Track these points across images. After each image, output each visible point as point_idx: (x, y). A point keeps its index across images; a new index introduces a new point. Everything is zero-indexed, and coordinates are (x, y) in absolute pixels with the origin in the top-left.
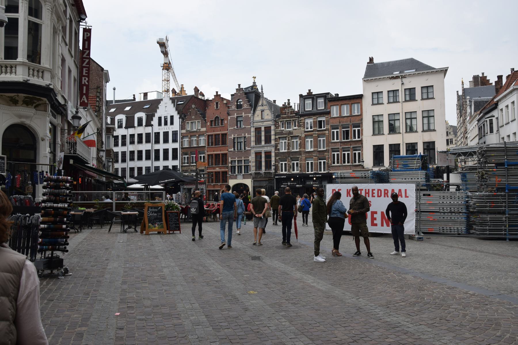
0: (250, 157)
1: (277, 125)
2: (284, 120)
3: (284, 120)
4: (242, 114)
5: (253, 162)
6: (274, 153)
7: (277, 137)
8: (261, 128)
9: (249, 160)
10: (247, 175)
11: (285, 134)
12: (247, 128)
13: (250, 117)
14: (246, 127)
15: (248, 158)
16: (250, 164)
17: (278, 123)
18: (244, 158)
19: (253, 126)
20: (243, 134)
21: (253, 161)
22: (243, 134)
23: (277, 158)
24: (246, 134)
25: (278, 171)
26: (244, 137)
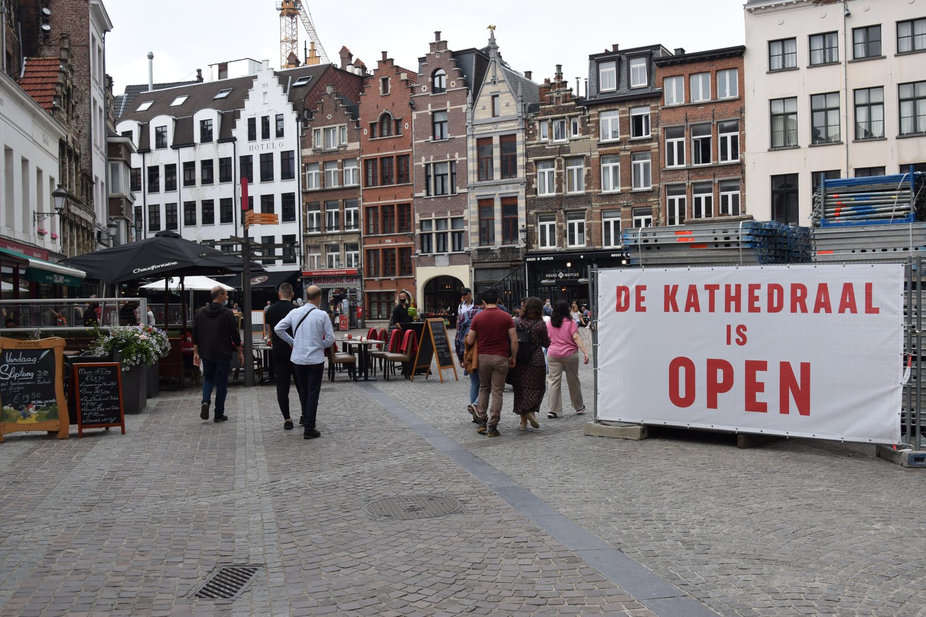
0: (466, 212)
1: (531, 129)
2: (547, 117)
3: (547, 117)
4: (446, 105)
5: (472, 223)
6: (524, 201)
7: (531, 160)
8: (492, 138)
9: (463, 218)
10: (459, 256)
11: (552, 152)
12: (459, 139)
13: (464, 111)
14: (456, 137)
15: (462, 213)
16: (466, 228)
17: (533, 124)
18: (451, 213)
19: (473, 135)
20: (448, 156)
21: (472, 220)
22: (448, 156)
23: (532, 213)
24: (457, 155)
25: (533, 246)
26: (451, 162)
